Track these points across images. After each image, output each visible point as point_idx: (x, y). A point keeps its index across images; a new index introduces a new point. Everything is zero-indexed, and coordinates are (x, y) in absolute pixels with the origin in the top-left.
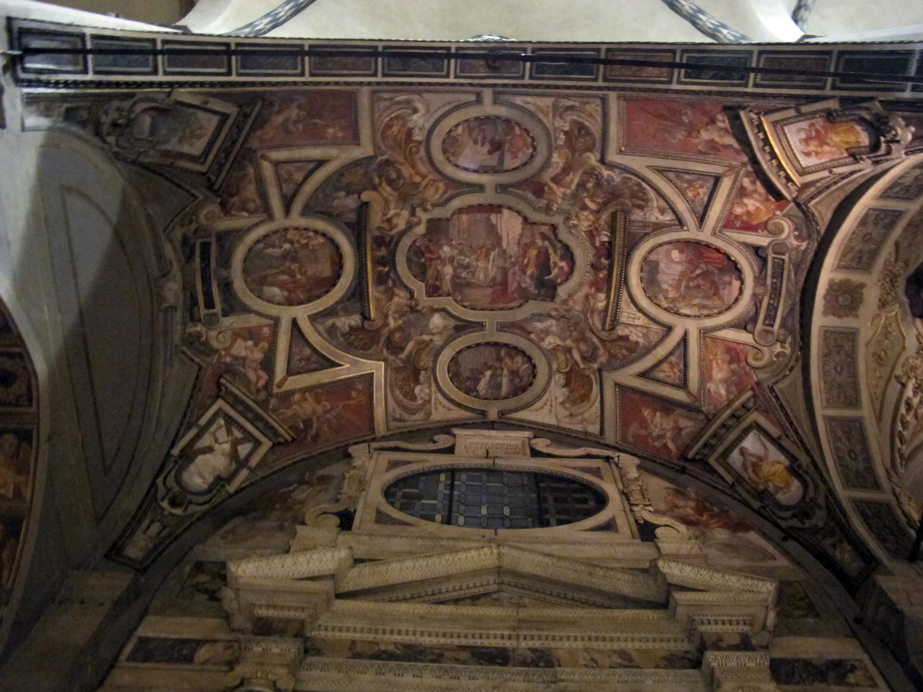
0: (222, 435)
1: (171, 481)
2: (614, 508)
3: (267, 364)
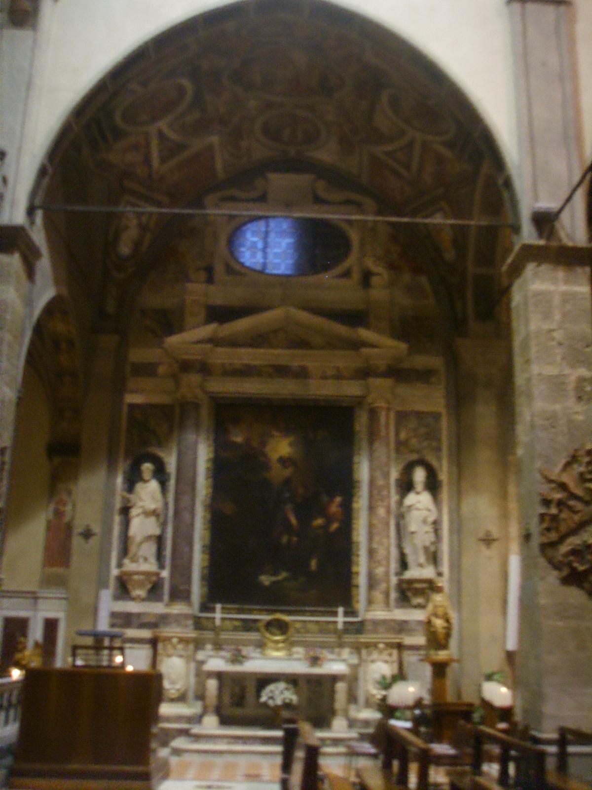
2: (351, 261)
3: (147, 162)
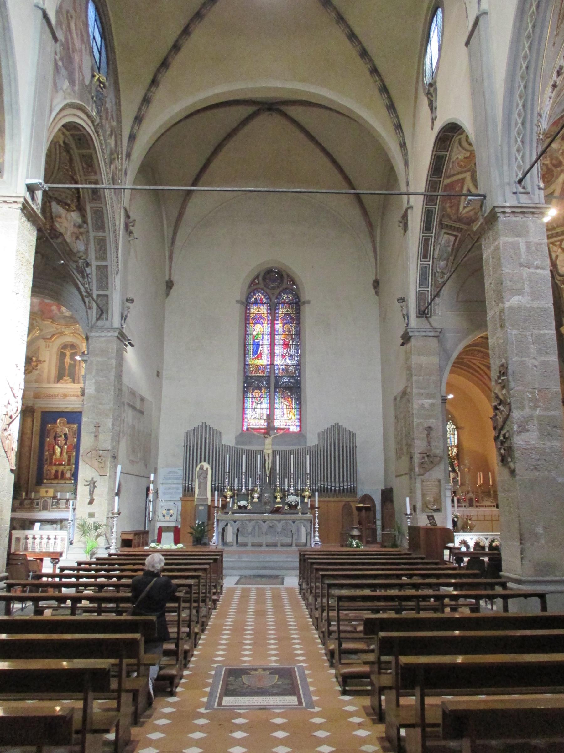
0: (555, 249)
1: (559, 278)
